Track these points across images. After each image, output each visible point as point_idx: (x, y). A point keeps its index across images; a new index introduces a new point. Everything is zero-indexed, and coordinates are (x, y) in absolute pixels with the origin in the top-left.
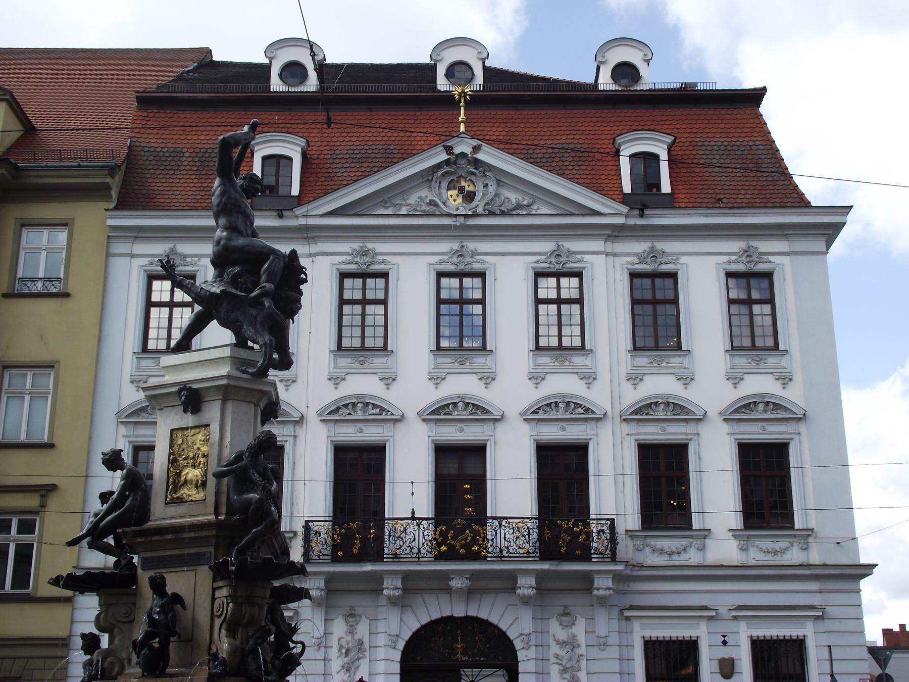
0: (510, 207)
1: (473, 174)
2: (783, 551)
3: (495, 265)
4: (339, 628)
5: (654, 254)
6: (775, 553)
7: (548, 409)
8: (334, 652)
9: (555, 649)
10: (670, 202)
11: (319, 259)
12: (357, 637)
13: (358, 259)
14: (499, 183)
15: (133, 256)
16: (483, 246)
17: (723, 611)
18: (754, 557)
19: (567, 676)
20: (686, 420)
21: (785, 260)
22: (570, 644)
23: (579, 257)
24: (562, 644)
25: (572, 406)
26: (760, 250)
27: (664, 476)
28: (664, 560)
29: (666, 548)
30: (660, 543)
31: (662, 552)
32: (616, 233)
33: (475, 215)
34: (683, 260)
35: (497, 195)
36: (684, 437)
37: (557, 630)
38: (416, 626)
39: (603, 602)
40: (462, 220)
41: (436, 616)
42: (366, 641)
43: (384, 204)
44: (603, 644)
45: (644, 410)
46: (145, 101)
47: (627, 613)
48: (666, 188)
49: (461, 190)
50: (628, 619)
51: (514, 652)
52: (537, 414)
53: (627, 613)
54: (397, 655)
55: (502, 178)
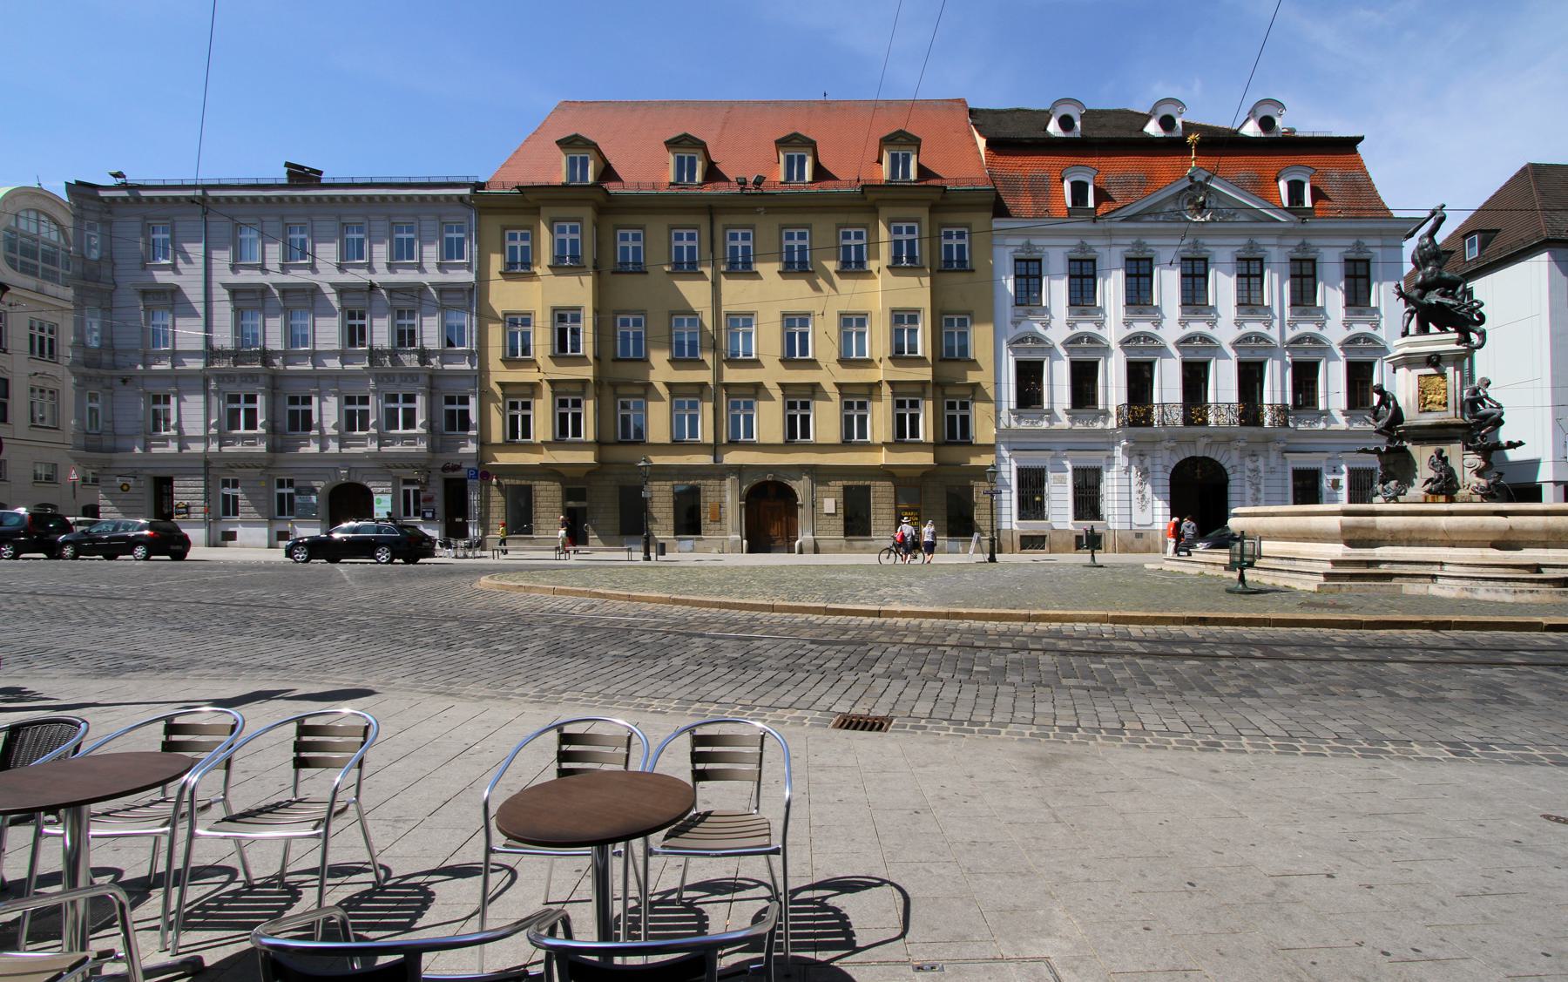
5: (1304, 246)
9: (1248, 473)
16: (1207, 241)
21: (1378, 251)
22: (1255, 470)
32: (1285, 233)
37: (1249, 463)
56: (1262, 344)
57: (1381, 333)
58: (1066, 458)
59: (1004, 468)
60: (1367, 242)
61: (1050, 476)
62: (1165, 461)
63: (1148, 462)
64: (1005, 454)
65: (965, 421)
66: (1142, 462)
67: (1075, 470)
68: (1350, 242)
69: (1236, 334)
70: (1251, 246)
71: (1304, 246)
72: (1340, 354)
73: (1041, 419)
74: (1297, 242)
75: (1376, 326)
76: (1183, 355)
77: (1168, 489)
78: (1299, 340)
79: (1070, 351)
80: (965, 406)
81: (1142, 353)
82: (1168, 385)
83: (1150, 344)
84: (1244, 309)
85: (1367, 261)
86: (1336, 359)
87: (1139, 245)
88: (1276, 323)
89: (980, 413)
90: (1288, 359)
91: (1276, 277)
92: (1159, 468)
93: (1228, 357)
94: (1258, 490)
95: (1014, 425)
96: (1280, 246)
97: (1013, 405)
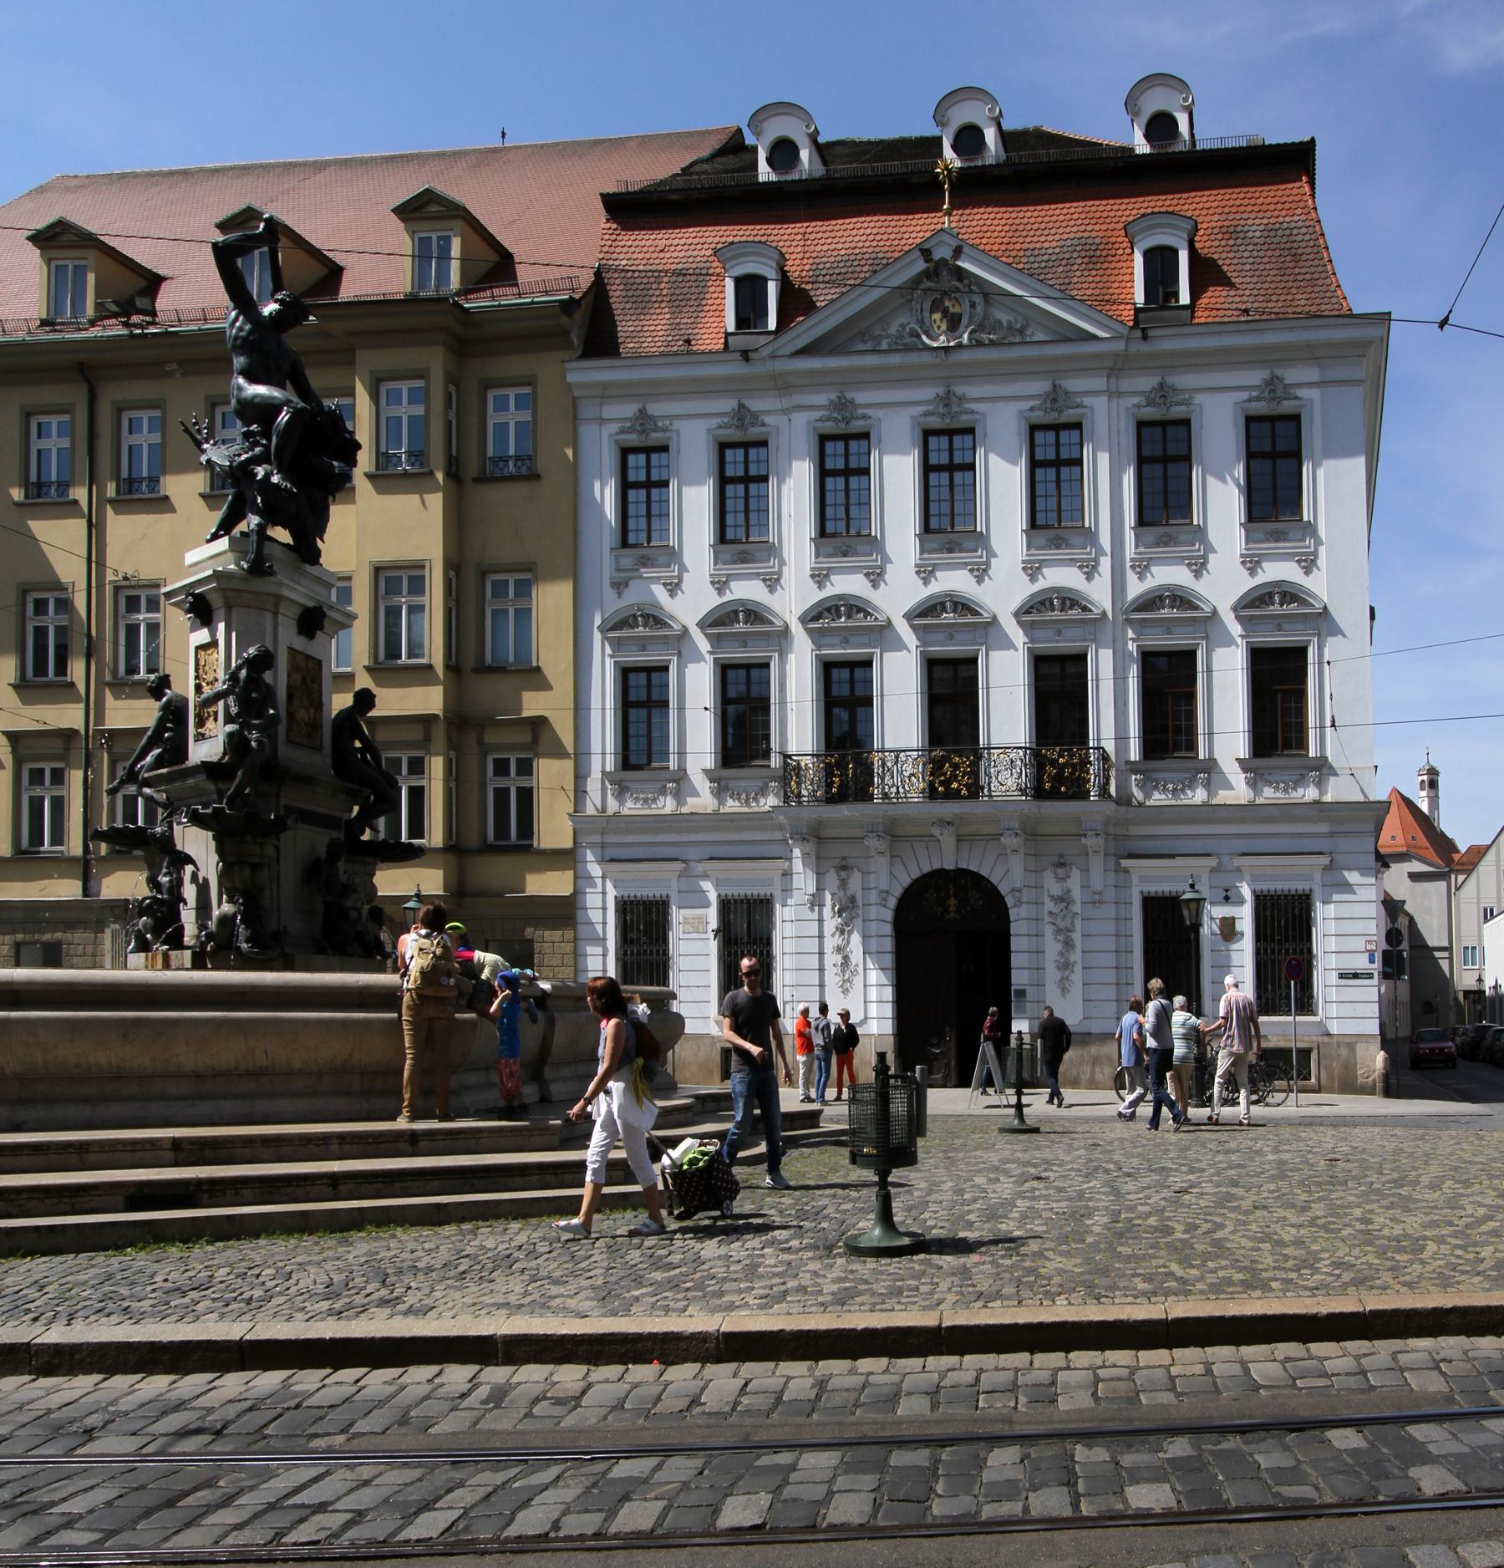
1: (958, 290)
3: (985, 415)
5: (1163, 393)
9: (1049, 905)
11: (795, 416)
13: (835, 415)
15: (603, 421)
19: (1061, 938)
21: (1314, 394)
22: (1064, 899)
24: (1058, 899)
26: (1287, 382)
34: (1199, 398)
38: (906, 881)
43: (862, 336)
44: (1097, 901)
48: (1184, 298)
51: (1006, 910)
54: (889, 915)
56: (1074, 613)
57: (1318, 585)
58: (706, 876)
59: (592, 900)
60: (1291, 375)
61: (677, 915)
62: (887, 879)
63: (855, 883)
64: (595, 870)
65: (526, 797)
66: (844, 884)
67: (727, 906)
68: (1255, 377)
69: (1023, 590)
70: (1054, 397)
71: (1163, 393)
72: (1236, 629)
73: (663, 791)
74: (1148, 383)
75: (1309, 564)
76: (923, 642)
77: (888, 944)
78: (1151, 602)
79: (716, 641)
80: (526, 768)
81: (845, 642)
82: (899, 718)
83: (859, 621)
84: (1042, 537)
85: (1296, 418)
86: (1229, 641)
88: (1105, 564)
89: (550, 774)
90: (1132, 647)
91: (1104, 459)
92: (873, 897)
93: (1009, 645)
94: (1068, 944)
95: (612, 805)
96: (1112, 394)
97: (610, 767)
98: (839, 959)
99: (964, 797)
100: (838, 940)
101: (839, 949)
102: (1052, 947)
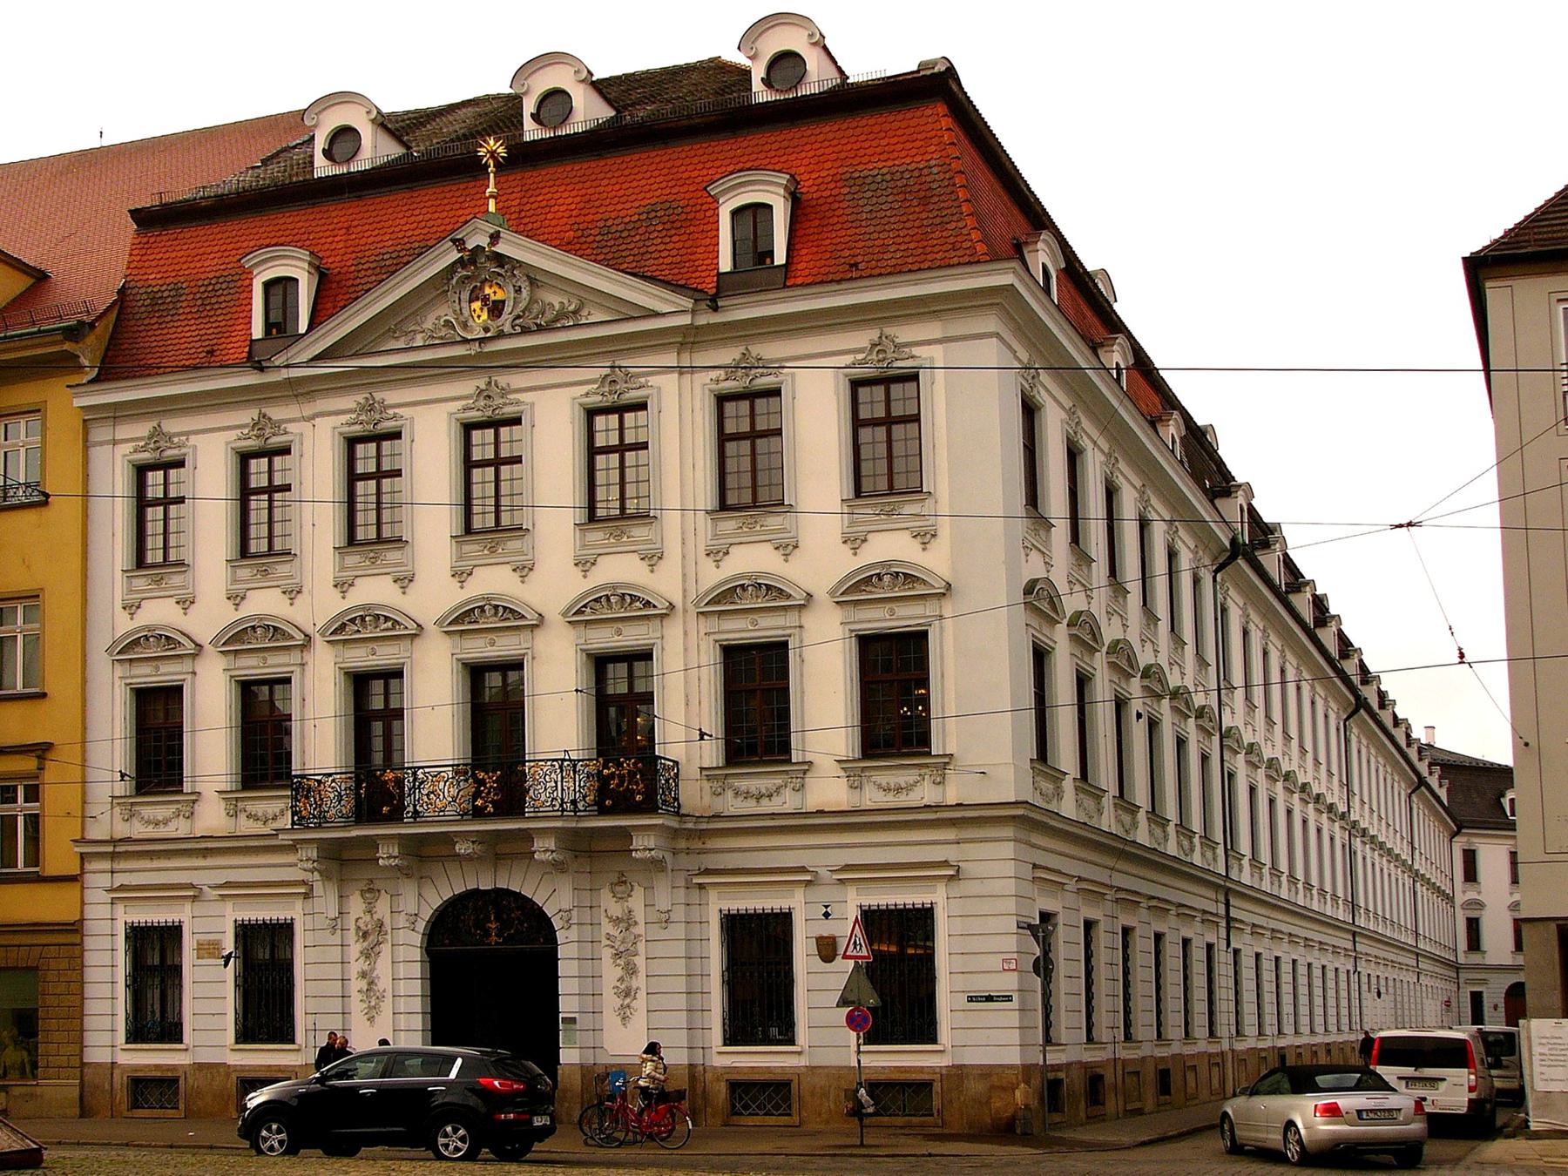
0: (549, 316)
2: (909, 788)
4: (356, 906)
6: (899, 789)
7: (597, 606)
8: (352, 936)
9: (607, 927)
10: (786, 278)
12: (376, 917)
14: (533, 282)
17: (823, 872)
18: (871, 797)
20: (784, 608)
22: (627, 921)
23: (643, 380)
24: (616, 921)
25: (628, 598)
27: (756, 690)
28: (750, 807)
29: (753, 790)
30: (743, 784)
31: (747, 795)
33: (501, 335)
35: (532, 301)
36: (780, 632)
39: (657, 865)
40: (475, 348)
41: (459, 889)
42: (387, 921)
45: (726, 597)
46: (148, 219)
47: (697, 880)
48: (780, 258)
49: (485, 299)
50: (701, 886)
52: (583, 613)
53: (697, 880)
55: (535, 278)
87: (369, 407)
94: (631, 970)
98: (363, 985)
99: (490, 815)
100: (361, 965)
101: (364, 975)
102: (611, 973)
